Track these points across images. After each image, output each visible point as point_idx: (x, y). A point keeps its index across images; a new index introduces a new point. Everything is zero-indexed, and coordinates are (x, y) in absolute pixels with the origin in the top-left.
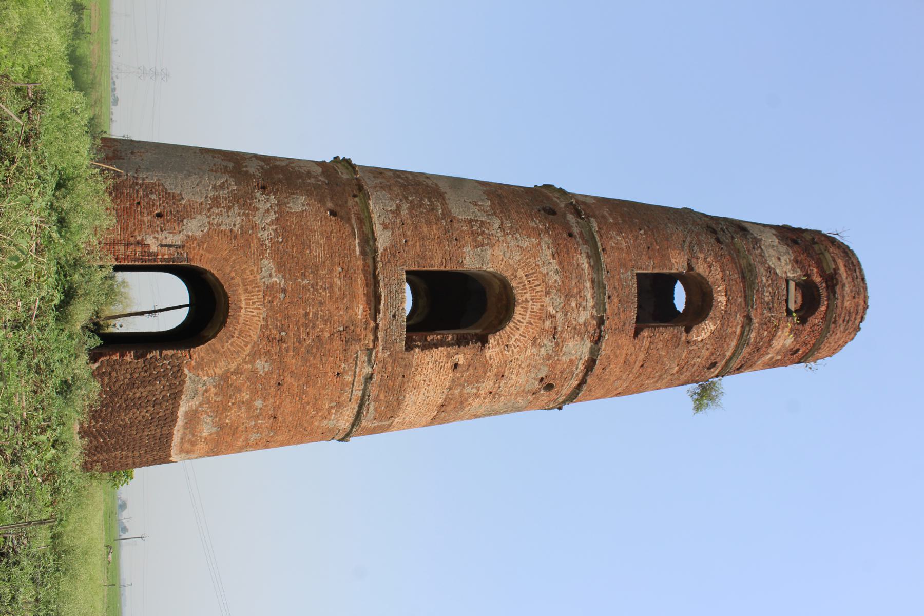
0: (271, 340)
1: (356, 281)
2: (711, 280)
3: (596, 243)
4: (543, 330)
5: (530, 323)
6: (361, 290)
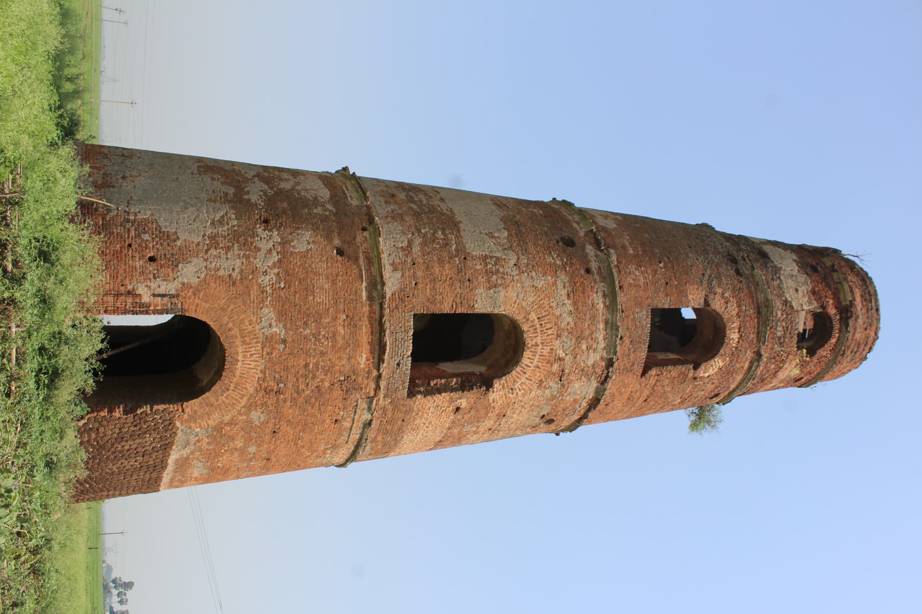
0: (267, 391)
1: (360, 329)
2: (726, 317)
3: (614, 281)
5: (538, 367)
6: (365, 338)
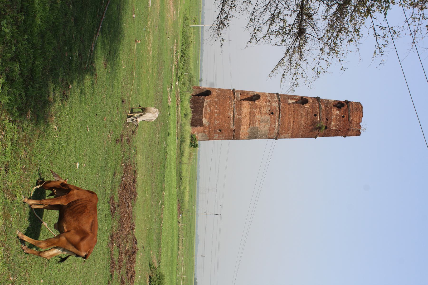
4: (267, 101)
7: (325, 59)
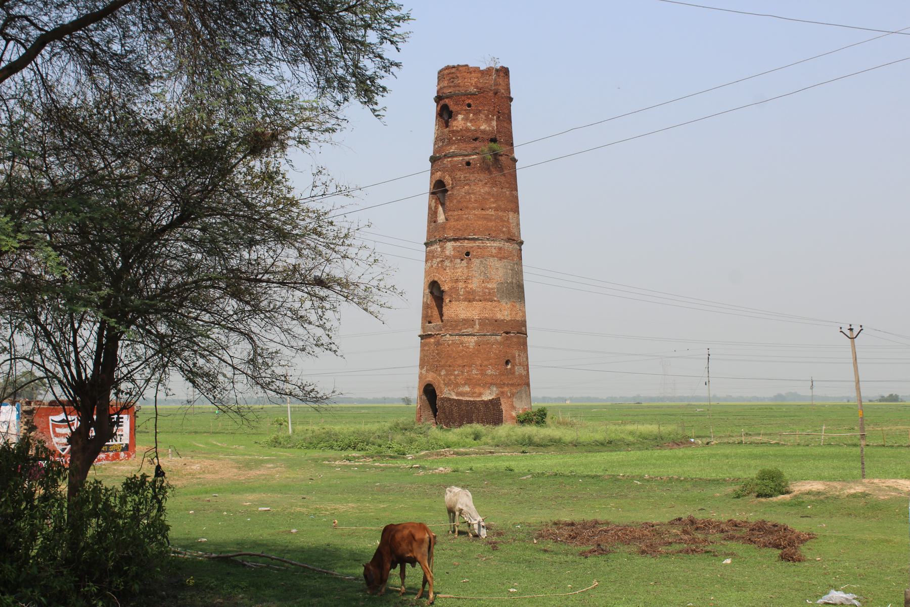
7: (356, 251)
